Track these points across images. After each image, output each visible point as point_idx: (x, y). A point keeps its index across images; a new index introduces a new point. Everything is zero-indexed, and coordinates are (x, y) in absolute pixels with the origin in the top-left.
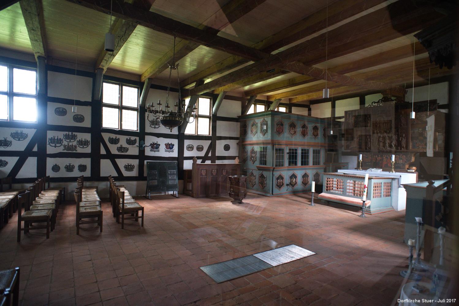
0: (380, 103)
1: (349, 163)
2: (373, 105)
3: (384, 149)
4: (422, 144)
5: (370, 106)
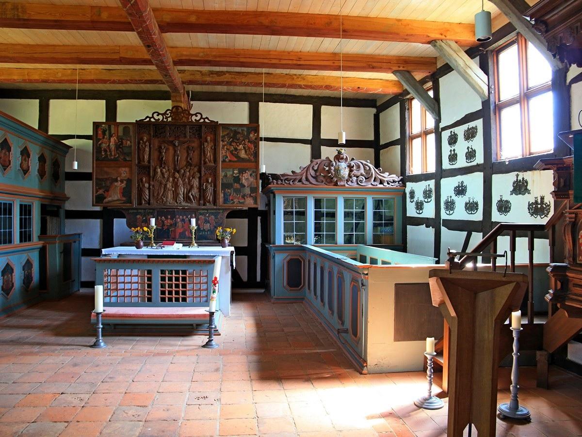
0: (169, 117)
1: (81, 234)
2: (154, 119)
3: (176, 205)
5: (148, 119)
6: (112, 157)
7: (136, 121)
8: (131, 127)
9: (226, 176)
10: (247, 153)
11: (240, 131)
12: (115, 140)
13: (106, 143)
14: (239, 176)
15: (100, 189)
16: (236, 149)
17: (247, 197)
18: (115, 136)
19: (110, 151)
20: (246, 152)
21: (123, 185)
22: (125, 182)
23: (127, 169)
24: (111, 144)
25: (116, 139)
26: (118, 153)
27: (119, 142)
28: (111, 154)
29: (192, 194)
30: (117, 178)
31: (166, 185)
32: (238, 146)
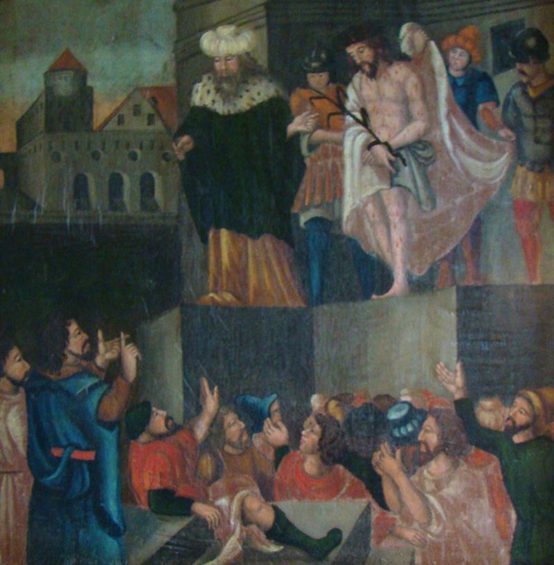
4: (277, 434)
14: (277, 112)
17: (416, 460)
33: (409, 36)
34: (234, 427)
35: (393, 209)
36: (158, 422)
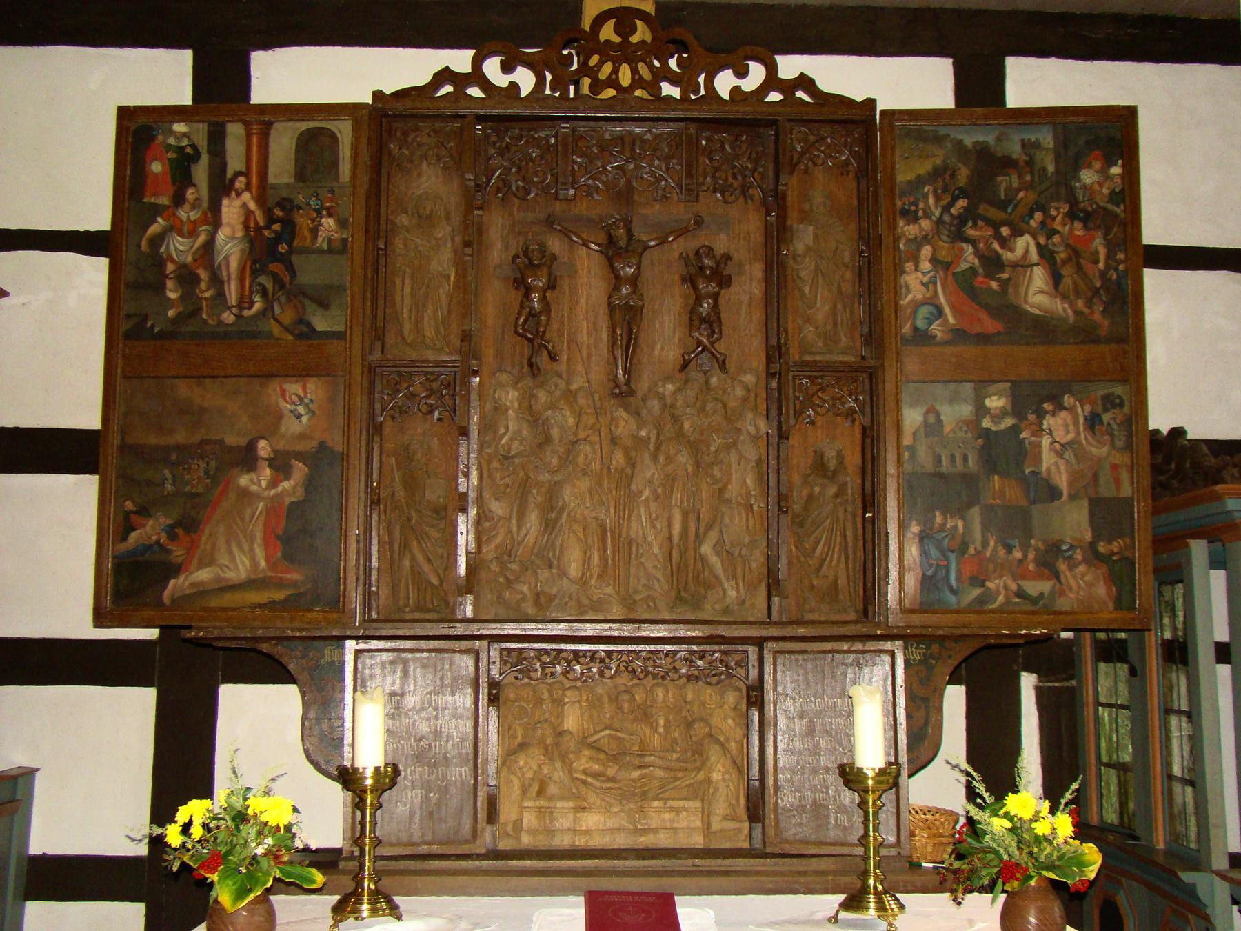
2: (485, 84)
4: (1018, 554)
6: (228, 317)
7: (377, 95)
8: (344, 129)
9: (932, 427)
10: (1067, 282)
11: (1014, 149)
12: (248, 214)
13: (193, 234)
15: (144, 511)
16: (992, 264)
17: (1072, 568)
18: (248, 188)
19: (217, 281)
20: (1056, 278)
21: (286, 485)
22: (300, 470)
23: (315, 389)
24: (221, 236)
25: (252, 206)
26: (264, 293)
27: (271, 220)
28: (221, 295)
29: (718, 547)
30: (251, 447)
31: (553, 492)
32: (1004, 242)
33: (1068, 400)
34: (1002, 552)
35: (1062, 468)
36: (972, 551)
